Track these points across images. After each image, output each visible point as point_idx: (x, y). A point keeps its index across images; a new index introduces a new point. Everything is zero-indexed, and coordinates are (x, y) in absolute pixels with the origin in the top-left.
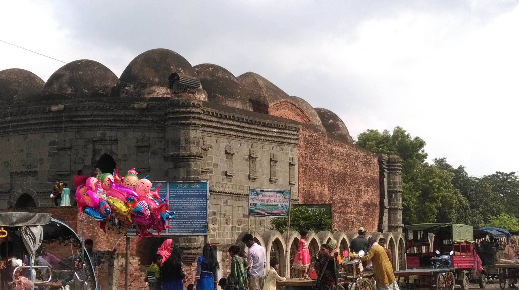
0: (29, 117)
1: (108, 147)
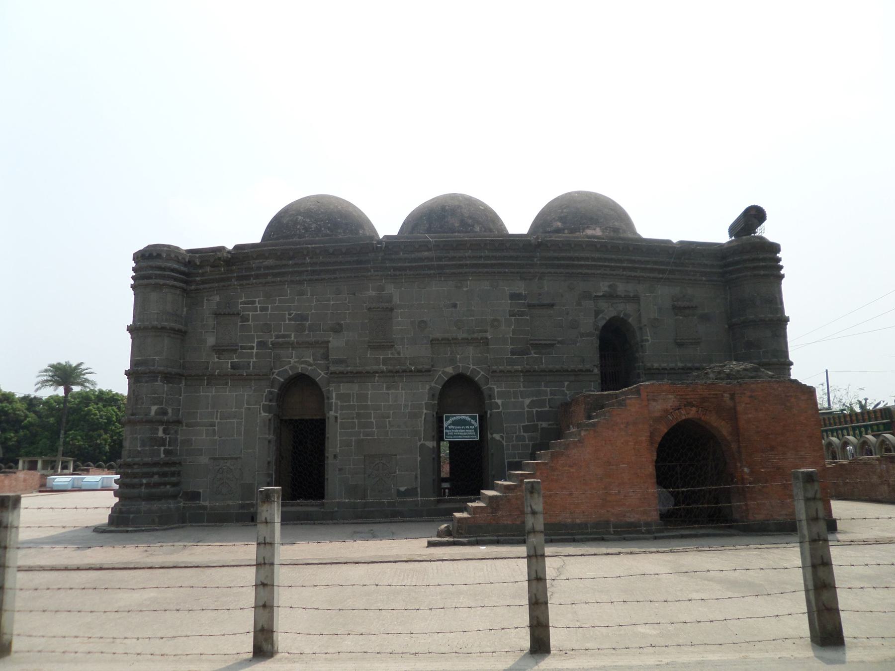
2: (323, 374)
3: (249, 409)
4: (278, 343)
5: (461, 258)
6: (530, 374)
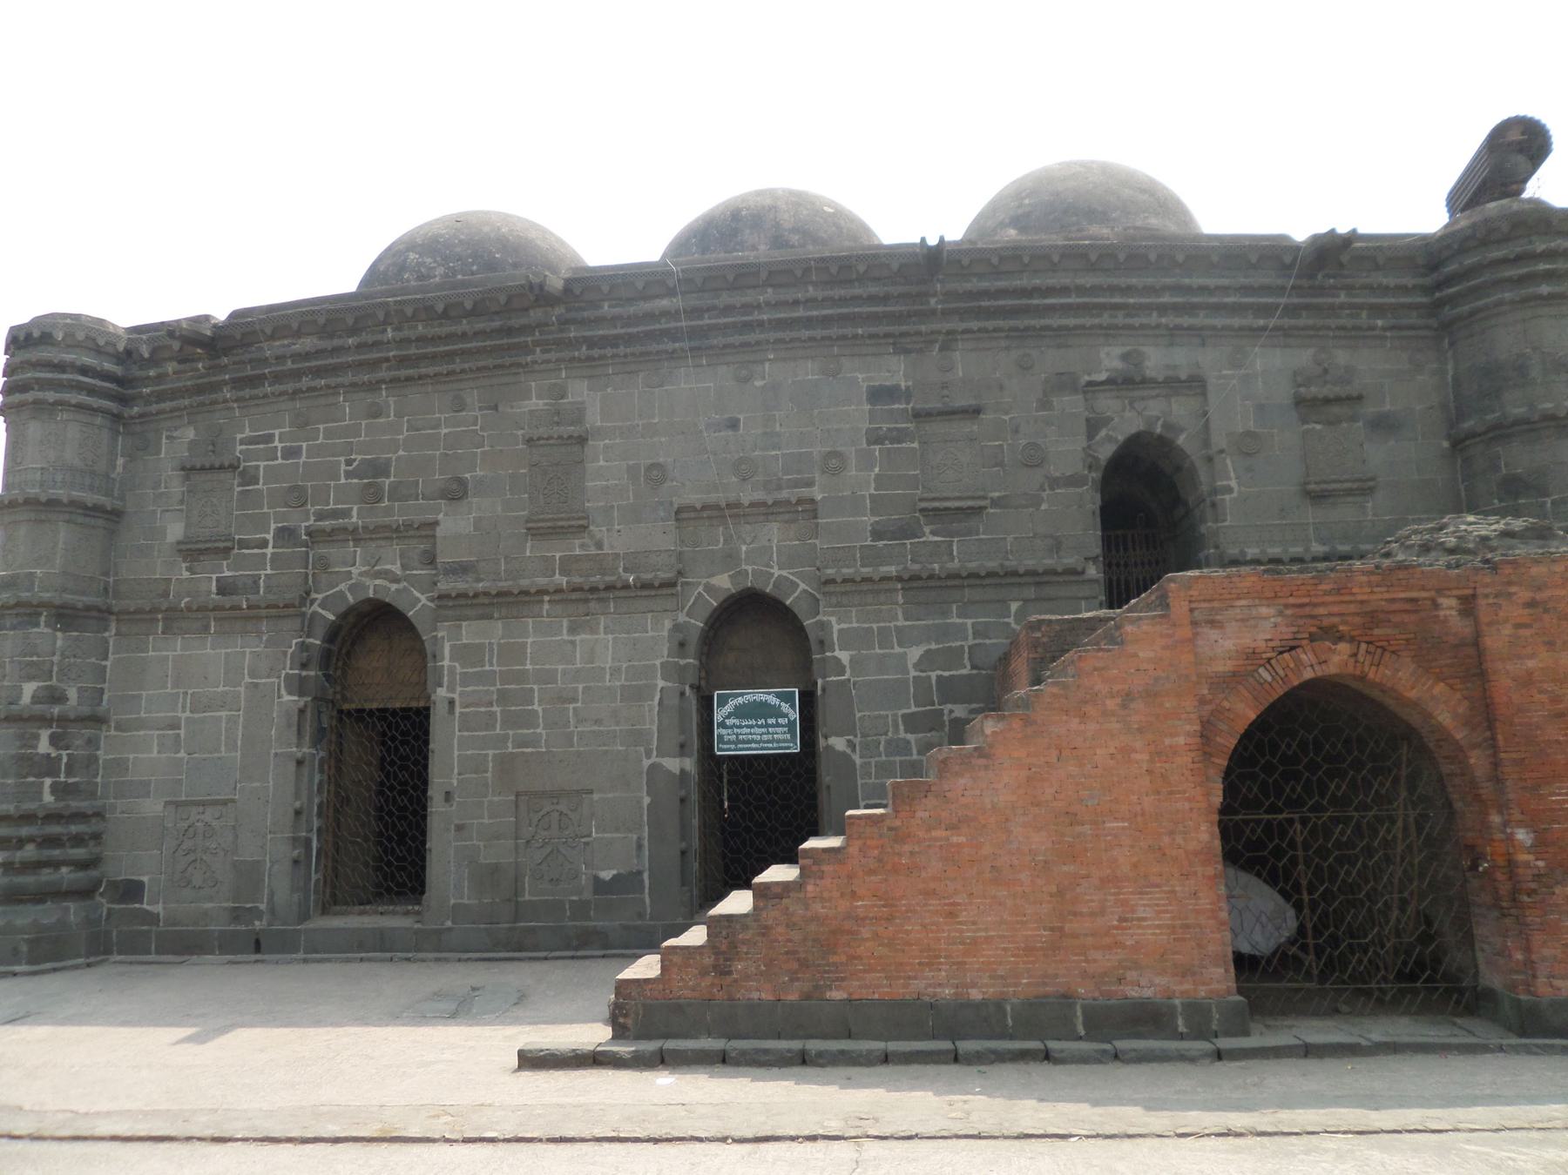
1: (1155, 408)
2: (423, 599)
3: (256, 685)
4: (322, 531)
5: (748, 308)
6: (923, 587)
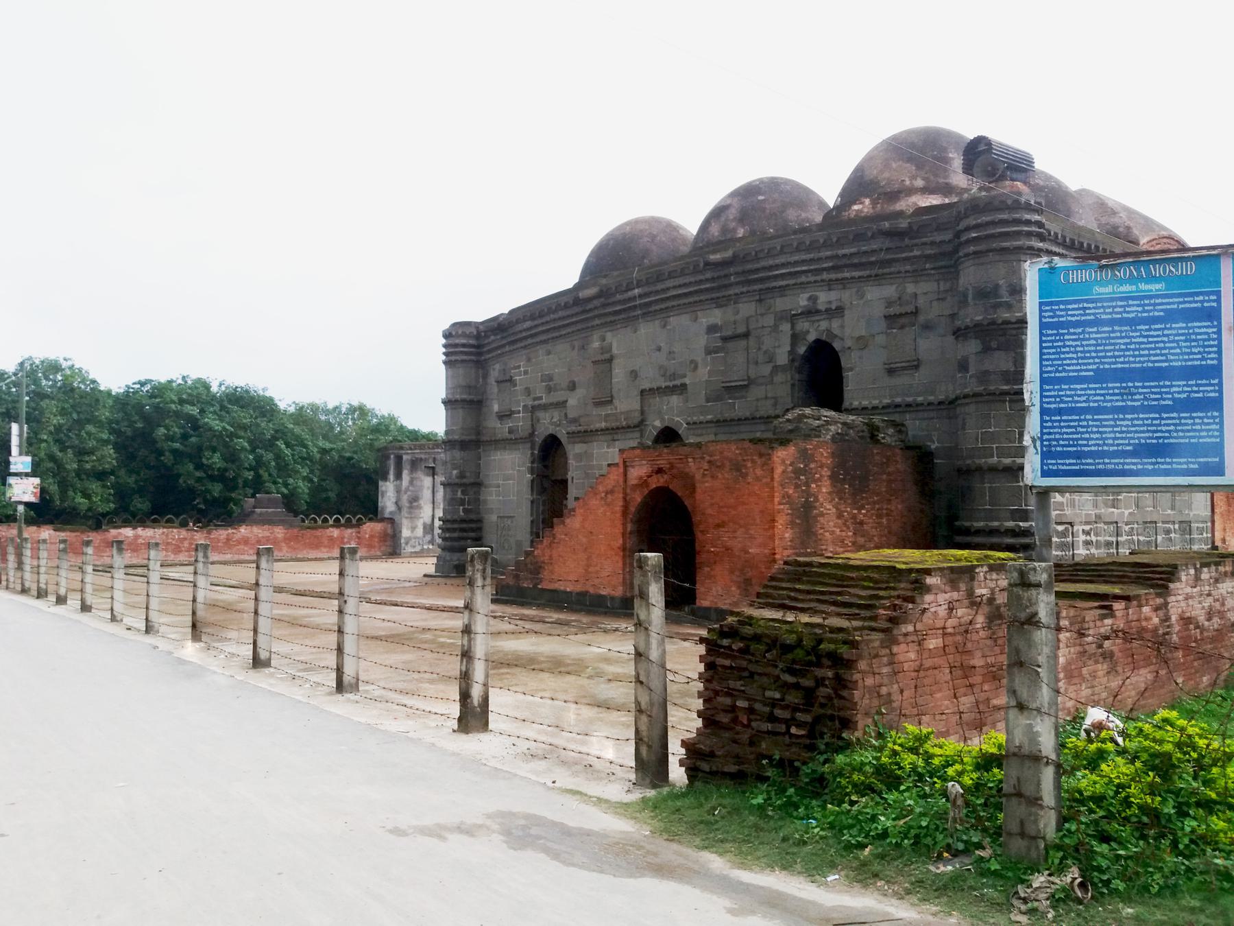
0: (670, 283)
1: (824, 325)
5: (664, 291)
